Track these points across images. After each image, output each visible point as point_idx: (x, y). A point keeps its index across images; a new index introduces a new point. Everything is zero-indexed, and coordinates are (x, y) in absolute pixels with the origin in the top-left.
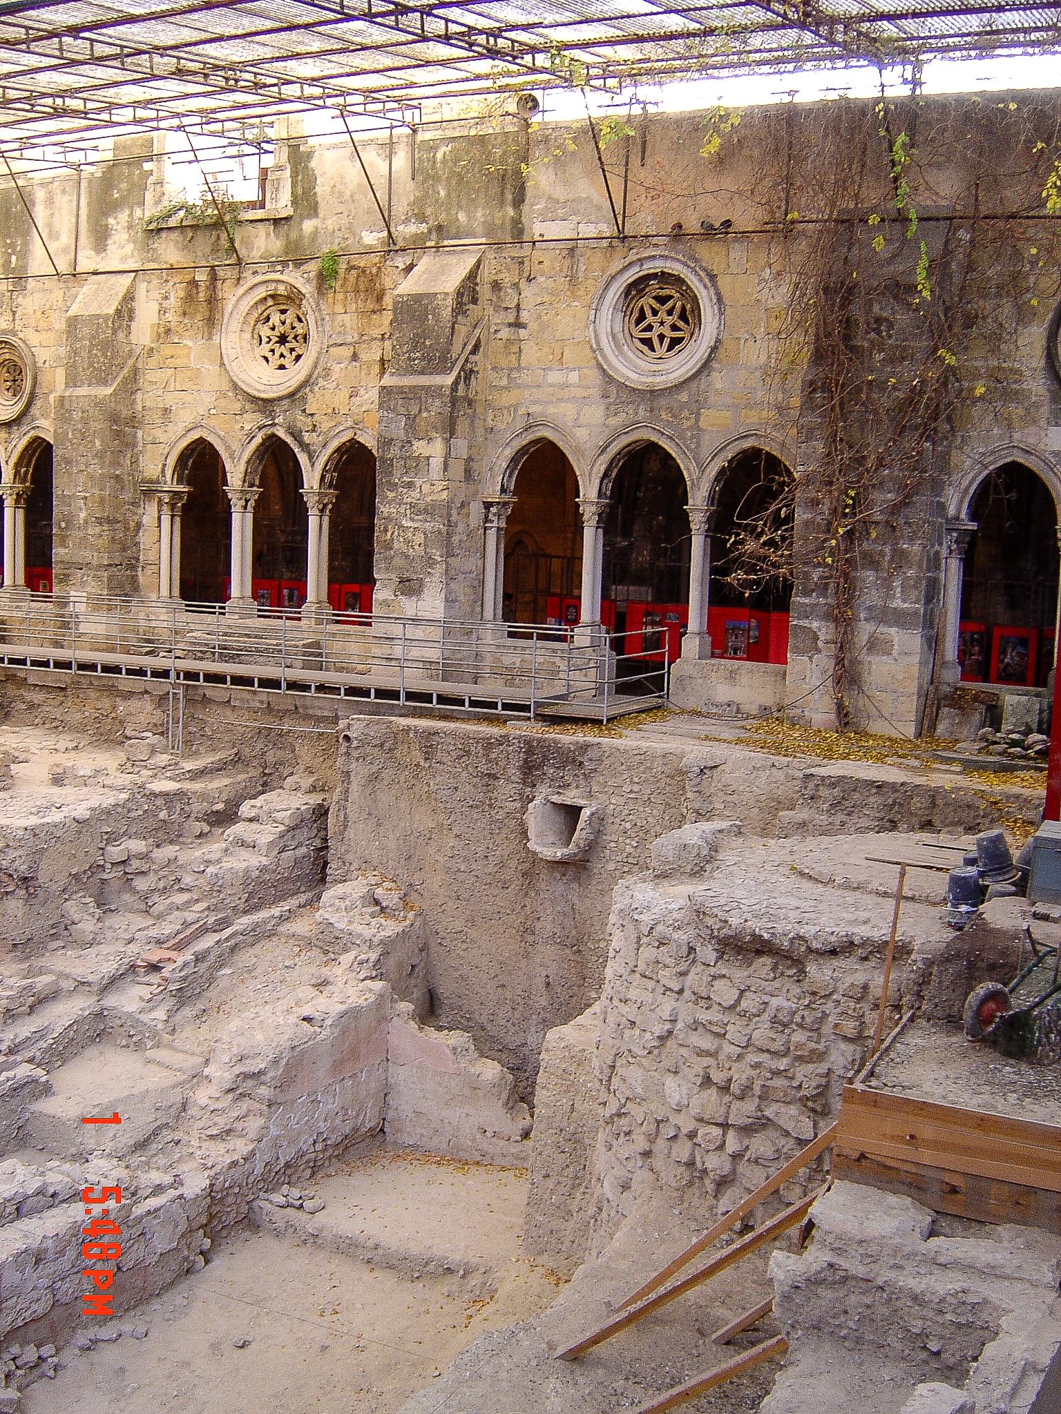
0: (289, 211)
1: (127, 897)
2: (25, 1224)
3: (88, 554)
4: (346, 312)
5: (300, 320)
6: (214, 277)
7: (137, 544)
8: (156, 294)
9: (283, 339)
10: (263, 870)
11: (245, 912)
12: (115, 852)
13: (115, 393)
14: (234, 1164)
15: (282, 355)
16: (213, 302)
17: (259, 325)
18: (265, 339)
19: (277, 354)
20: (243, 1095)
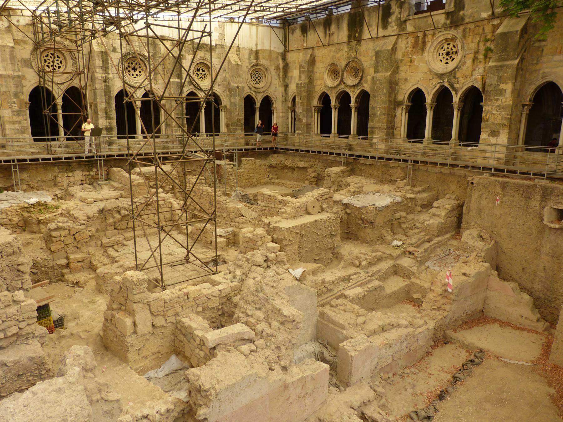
0: (453, 9)
1: (399, 229)
2: (387, 334)
3: (380, 124)
4: (473, 42)
5: (454, 47)
6: (425, 35)
7: (394, 121)
8: (404, 42)
9: (448, 54)
10: (442, 223)
11: (437, 237)
12: (397, 215)
13: (391, 74)
14: (442, 318)
15: (447, 59)
16: (424, 43)
17: (440, 50)
18: (441, 54)
19: (445, 58)
20: (444, 297)
